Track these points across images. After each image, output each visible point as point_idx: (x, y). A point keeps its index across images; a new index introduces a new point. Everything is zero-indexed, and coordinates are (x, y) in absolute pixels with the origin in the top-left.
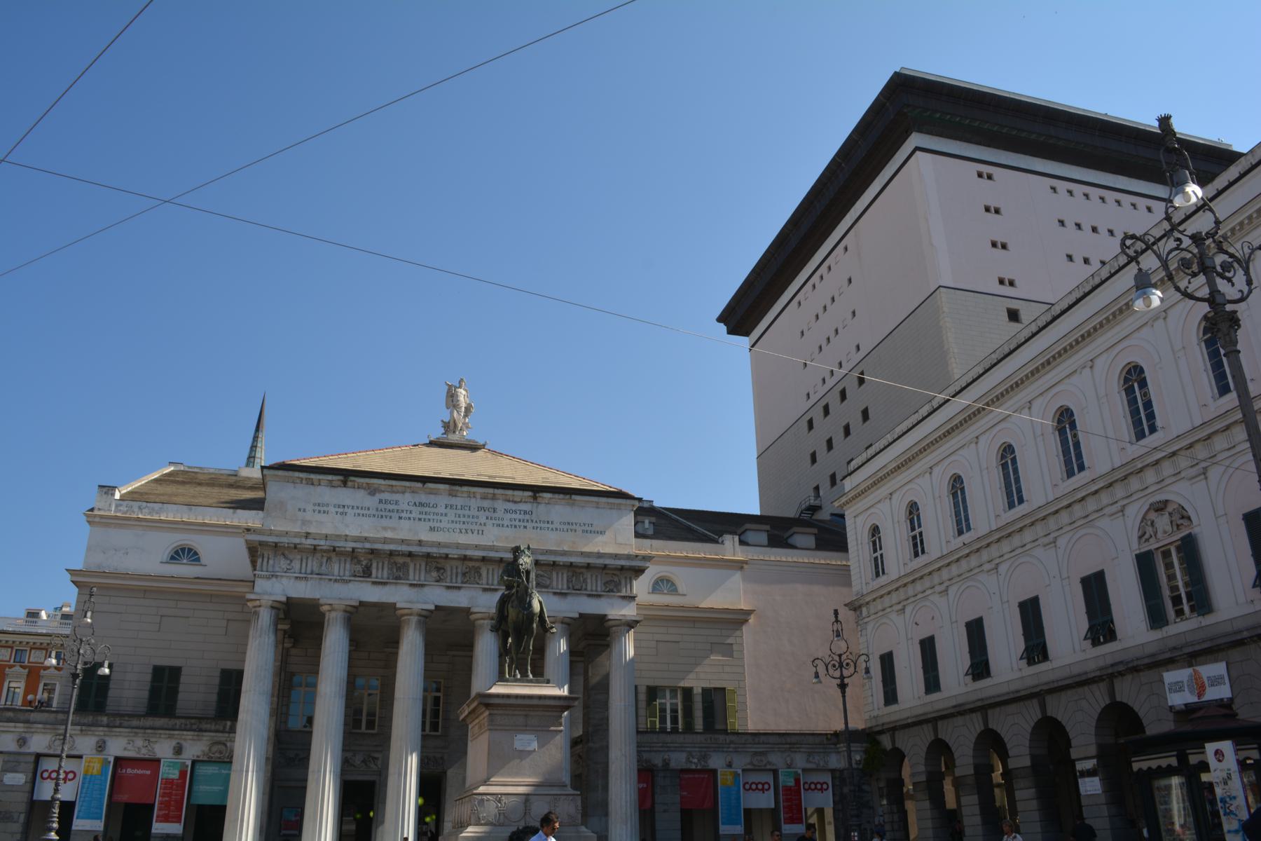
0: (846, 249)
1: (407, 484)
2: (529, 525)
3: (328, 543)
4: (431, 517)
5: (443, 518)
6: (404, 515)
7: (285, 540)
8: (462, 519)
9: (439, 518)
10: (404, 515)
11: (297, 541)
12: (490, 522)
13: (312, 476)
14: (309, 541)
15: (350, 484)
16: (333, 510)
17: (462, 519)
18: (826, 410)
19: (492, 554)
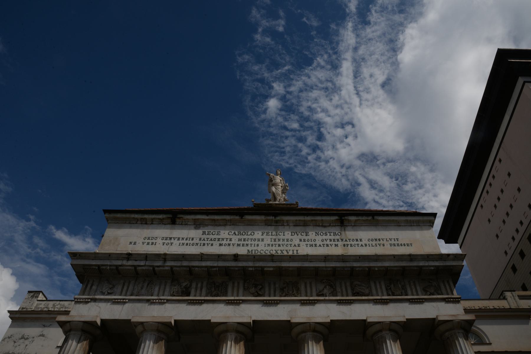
0: (500, 161)
1: (228, 217)
2: (340, 243)
3: (148, 263)
4: (249, 242)
5: (260, 243)
6: (224, 242)
7: (108, 263)
8: (277, 243)
9: (256, 243)
10: (224, 242)
11: (119, 263)
12: (302, 243)
13: (146, 216)
14: (130, 263)
15: (178, 221)
16: (159, 241)
17: (277, 243)
18: (522, 254)
19: (306, 264)
